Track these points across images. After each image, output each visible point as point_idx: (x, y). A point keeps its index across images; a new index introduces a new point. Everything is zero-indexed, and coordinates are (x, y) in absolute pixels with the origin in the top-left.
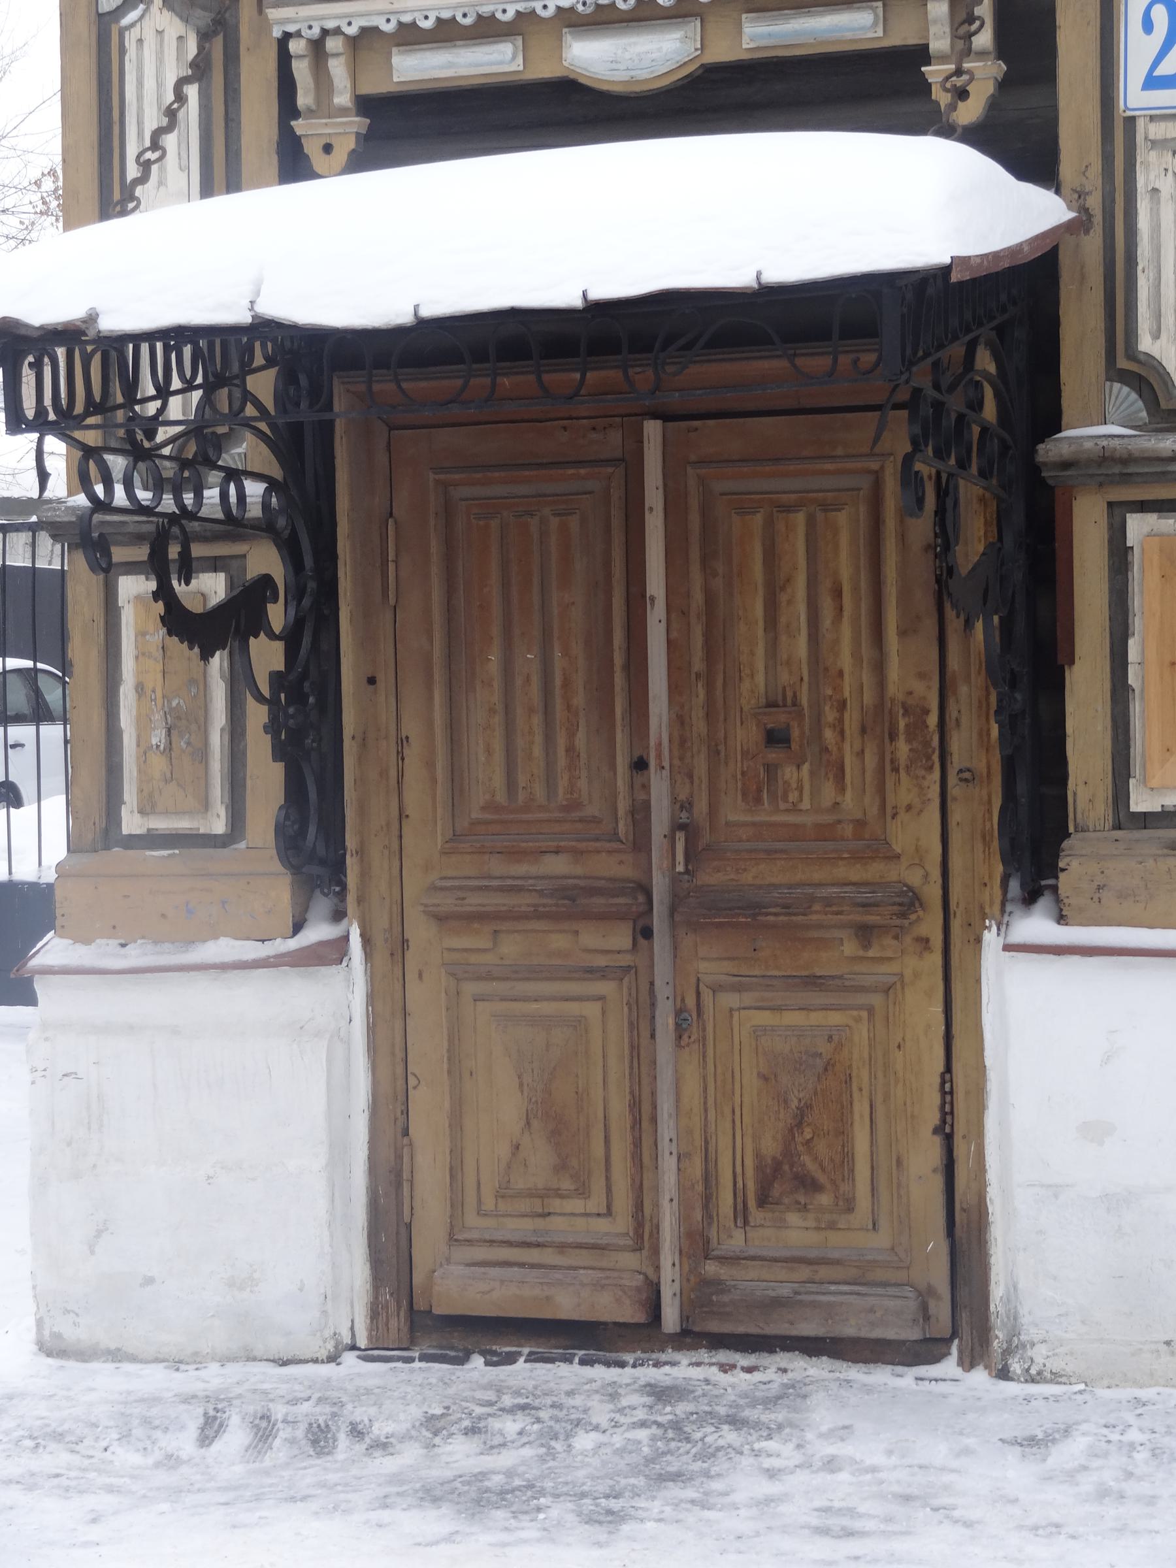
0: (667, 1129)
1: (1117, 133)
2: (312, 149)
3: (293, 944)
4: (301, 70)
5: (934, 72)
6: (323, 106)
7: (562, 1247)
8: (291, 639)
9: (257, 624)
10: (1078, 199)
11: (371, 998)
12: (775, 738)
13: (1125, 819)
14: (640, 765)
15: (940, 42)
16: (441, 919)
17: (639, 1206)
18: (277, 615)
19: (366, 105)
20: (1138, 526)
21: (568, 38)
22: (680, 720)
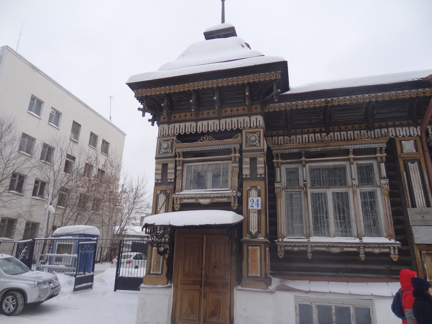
0: (202, 308)
1: (248, 211)
2: (175, 208)
3: (166, 286)
4: (175, 201)
5: (232, 204)
6: (177, 204)
7: (191, 320)
8: (169, 254)
9: (166, 253)
10: (244, 217)
11: (174, 292)
12: (215, 267)
13: (248, 277)
14: (202, 269)
15: (232, 202)
16: (182, 284)
17: (199, 316)
18: (168, 252)
19: (180, 204)
20: (250, 247)
22: (206, 264)
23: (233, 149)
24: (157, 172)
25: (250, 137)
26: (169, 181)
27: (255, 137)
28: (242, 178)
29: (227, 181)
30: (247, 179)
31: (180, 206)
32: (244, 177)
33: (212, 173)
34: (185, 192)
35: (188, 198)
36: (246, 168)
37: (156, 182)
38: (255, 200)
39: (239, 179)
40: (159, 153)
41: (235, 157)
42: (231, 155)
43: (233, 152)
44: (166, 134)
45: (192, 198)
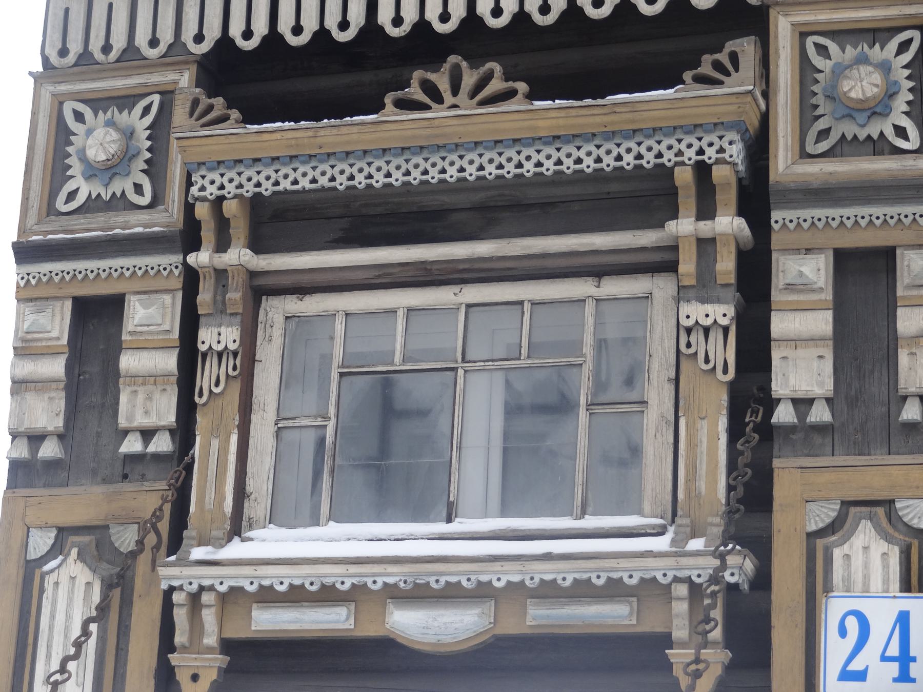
4: (180, 616)
5: (678, 656)
15: (680, 632)
19: (228, 646)
21: (390, 607)
23: (684, 177)
24: (29, 368)
25: (840, 71)
26: (132, 445)
27: (885, 68)
28: (767, 431)
29: (636, 451)
30: (809, 436)
31: (221, 660)
32: (784, 414)
33: (499, 377)
34: (268, 543)
35: (296, 596)
36: (796, 342)
37: (23, 452)
38: (882, 614)
39: (735, 432)
40: (51, 210)
41: (706, 246)
42: (671, 226)
43: (687, 202)
44: (107, 48)
45: (328, 595)
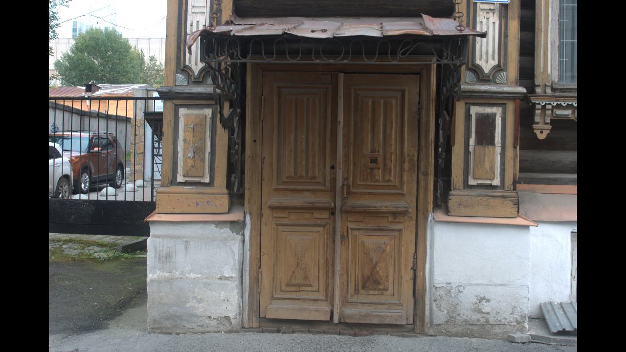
22: (346, 156)
